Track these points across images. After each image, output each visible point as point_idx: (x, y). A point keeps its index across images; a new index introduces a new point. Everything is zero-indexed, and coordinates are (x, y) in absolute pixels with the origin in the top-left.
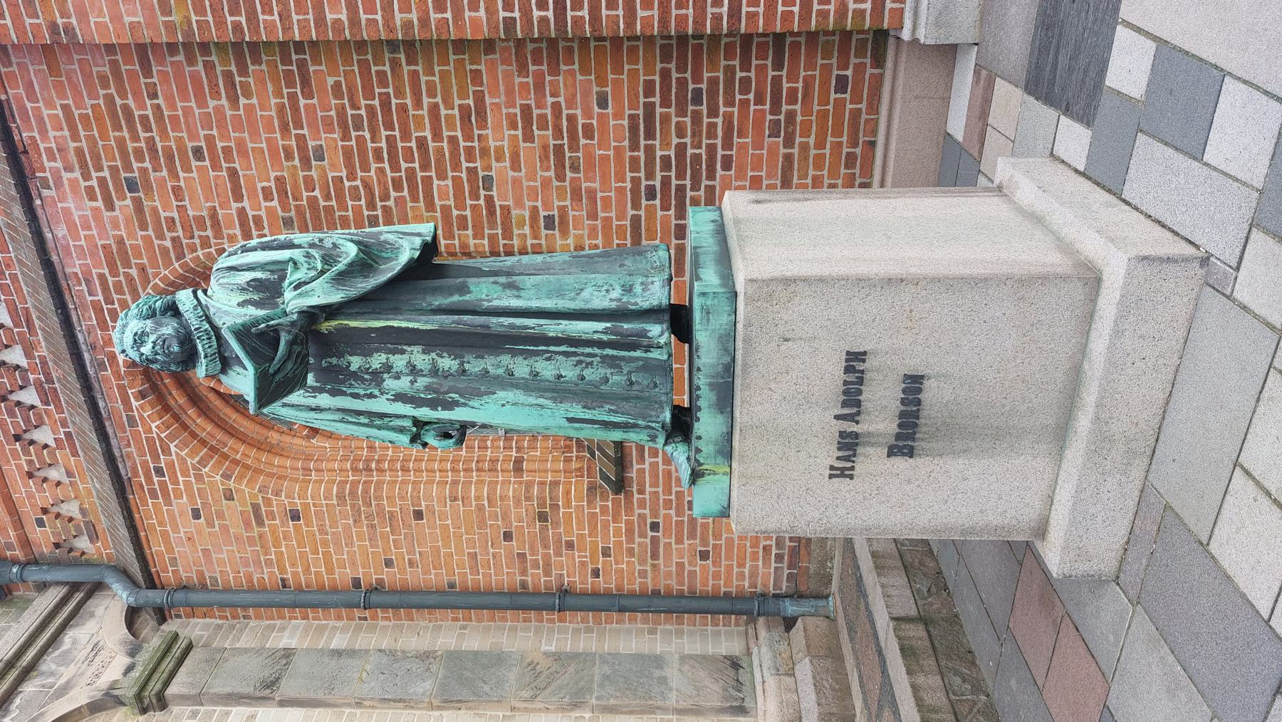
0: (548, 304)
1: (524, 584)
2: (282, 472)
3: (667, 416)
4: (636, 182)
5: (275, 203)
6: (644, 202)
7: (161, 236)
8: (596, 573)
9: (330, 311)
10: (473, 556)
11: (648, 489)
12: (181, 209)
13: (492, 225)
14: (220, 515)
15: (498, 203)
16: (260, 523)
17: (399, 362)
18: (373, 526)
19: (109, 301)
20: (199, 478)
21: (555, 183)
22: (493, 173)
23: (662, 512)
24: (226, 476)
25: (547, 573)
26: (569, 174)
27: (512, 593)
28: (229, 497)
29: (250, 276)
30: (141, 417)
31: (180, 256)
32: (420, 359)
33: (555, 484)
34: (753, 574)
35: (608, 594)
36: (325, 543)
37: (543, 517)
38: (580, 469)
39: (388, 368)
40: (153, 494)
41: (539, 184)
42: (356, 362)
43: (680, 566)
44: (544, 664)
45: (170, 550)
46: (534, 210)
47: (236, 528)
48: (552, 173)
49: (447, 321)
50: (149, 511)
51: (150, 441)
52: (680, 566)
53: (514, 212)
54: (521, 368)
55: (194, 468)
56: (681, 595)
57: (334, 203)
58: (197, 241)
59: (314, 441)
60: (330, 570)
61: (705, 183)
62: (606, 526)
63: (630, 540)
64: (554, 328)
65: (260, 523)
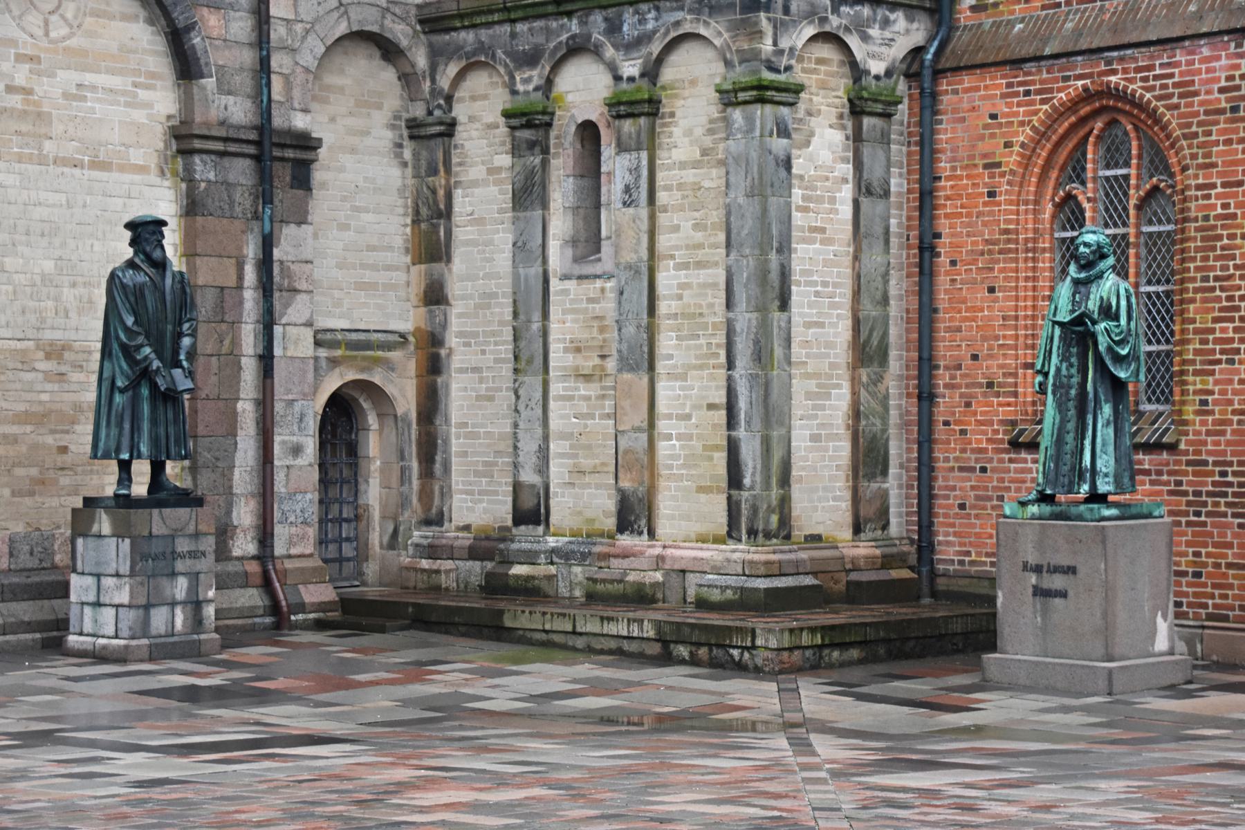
0: (1099, 440)
1: (937, 367)
2: (1026, 184)
3: (1049, 492)
4: (1231, 464)
5: (1219, 211)
6: (1217, 469)
7: (1200, 124)
8: (946, 423)
9: (1096, 344)
10: (959, 330)
11: (1012, 466)
12: (1217, 143)
13: (1202, 363)
14: (993, 136)
15: (1217, 367)
16: (986, 166)
17: (1074, 371)
18: (982, 254)
19: (1156, 78)
20: (1022, 124)
21: (1230, 409)
22: (1236, 366)
23: (996, 476)
24: (1023, 145)
25: (946, 386)
26: (1236, 418)
27: (931, 358)
28: (1008, 145)
29: (1114, 304)
30: (1069, 87)
31: (1185, 136)
32: (1075, 380)
33: (1015, 394)
34: (948, 543)
35: (931, 432)
36: (969, 215)
37: (990, 385)
38: (1027, 414)
39: (1071, 365)
40: (1009, 85)
41: (1230, 397)
42: (1074, 350)
43: (954, 488)
44: (881, 387)
45: (966, 90)
46: (1211, 393)
47: (982, 147)
48: (1236, 406)
49: (1091, 396)
50: (997, 81)
51: (1051, 91)
52: (954, 488)
53: (1211, 379)
54: (1071, 426)
55: (1030, 122)
56: (931, 488)
57: (1219, 252)
58: (1195, 150)
59: (1050, 206)
60: (947, 216)
61: (1230, 511)
62: (984, 433)
63: (973, 451)
64: (1087, 443)
65: (986, 166)
